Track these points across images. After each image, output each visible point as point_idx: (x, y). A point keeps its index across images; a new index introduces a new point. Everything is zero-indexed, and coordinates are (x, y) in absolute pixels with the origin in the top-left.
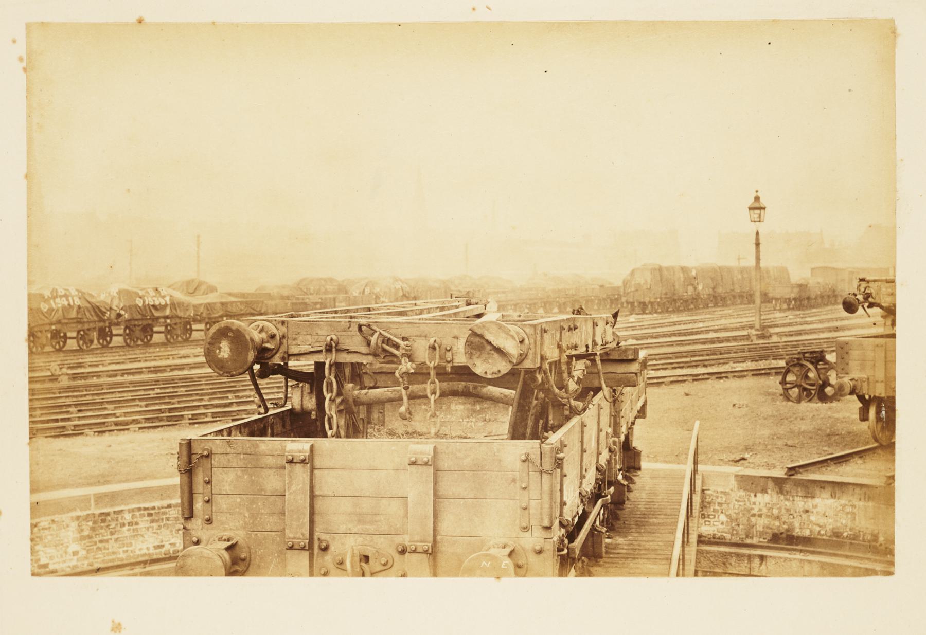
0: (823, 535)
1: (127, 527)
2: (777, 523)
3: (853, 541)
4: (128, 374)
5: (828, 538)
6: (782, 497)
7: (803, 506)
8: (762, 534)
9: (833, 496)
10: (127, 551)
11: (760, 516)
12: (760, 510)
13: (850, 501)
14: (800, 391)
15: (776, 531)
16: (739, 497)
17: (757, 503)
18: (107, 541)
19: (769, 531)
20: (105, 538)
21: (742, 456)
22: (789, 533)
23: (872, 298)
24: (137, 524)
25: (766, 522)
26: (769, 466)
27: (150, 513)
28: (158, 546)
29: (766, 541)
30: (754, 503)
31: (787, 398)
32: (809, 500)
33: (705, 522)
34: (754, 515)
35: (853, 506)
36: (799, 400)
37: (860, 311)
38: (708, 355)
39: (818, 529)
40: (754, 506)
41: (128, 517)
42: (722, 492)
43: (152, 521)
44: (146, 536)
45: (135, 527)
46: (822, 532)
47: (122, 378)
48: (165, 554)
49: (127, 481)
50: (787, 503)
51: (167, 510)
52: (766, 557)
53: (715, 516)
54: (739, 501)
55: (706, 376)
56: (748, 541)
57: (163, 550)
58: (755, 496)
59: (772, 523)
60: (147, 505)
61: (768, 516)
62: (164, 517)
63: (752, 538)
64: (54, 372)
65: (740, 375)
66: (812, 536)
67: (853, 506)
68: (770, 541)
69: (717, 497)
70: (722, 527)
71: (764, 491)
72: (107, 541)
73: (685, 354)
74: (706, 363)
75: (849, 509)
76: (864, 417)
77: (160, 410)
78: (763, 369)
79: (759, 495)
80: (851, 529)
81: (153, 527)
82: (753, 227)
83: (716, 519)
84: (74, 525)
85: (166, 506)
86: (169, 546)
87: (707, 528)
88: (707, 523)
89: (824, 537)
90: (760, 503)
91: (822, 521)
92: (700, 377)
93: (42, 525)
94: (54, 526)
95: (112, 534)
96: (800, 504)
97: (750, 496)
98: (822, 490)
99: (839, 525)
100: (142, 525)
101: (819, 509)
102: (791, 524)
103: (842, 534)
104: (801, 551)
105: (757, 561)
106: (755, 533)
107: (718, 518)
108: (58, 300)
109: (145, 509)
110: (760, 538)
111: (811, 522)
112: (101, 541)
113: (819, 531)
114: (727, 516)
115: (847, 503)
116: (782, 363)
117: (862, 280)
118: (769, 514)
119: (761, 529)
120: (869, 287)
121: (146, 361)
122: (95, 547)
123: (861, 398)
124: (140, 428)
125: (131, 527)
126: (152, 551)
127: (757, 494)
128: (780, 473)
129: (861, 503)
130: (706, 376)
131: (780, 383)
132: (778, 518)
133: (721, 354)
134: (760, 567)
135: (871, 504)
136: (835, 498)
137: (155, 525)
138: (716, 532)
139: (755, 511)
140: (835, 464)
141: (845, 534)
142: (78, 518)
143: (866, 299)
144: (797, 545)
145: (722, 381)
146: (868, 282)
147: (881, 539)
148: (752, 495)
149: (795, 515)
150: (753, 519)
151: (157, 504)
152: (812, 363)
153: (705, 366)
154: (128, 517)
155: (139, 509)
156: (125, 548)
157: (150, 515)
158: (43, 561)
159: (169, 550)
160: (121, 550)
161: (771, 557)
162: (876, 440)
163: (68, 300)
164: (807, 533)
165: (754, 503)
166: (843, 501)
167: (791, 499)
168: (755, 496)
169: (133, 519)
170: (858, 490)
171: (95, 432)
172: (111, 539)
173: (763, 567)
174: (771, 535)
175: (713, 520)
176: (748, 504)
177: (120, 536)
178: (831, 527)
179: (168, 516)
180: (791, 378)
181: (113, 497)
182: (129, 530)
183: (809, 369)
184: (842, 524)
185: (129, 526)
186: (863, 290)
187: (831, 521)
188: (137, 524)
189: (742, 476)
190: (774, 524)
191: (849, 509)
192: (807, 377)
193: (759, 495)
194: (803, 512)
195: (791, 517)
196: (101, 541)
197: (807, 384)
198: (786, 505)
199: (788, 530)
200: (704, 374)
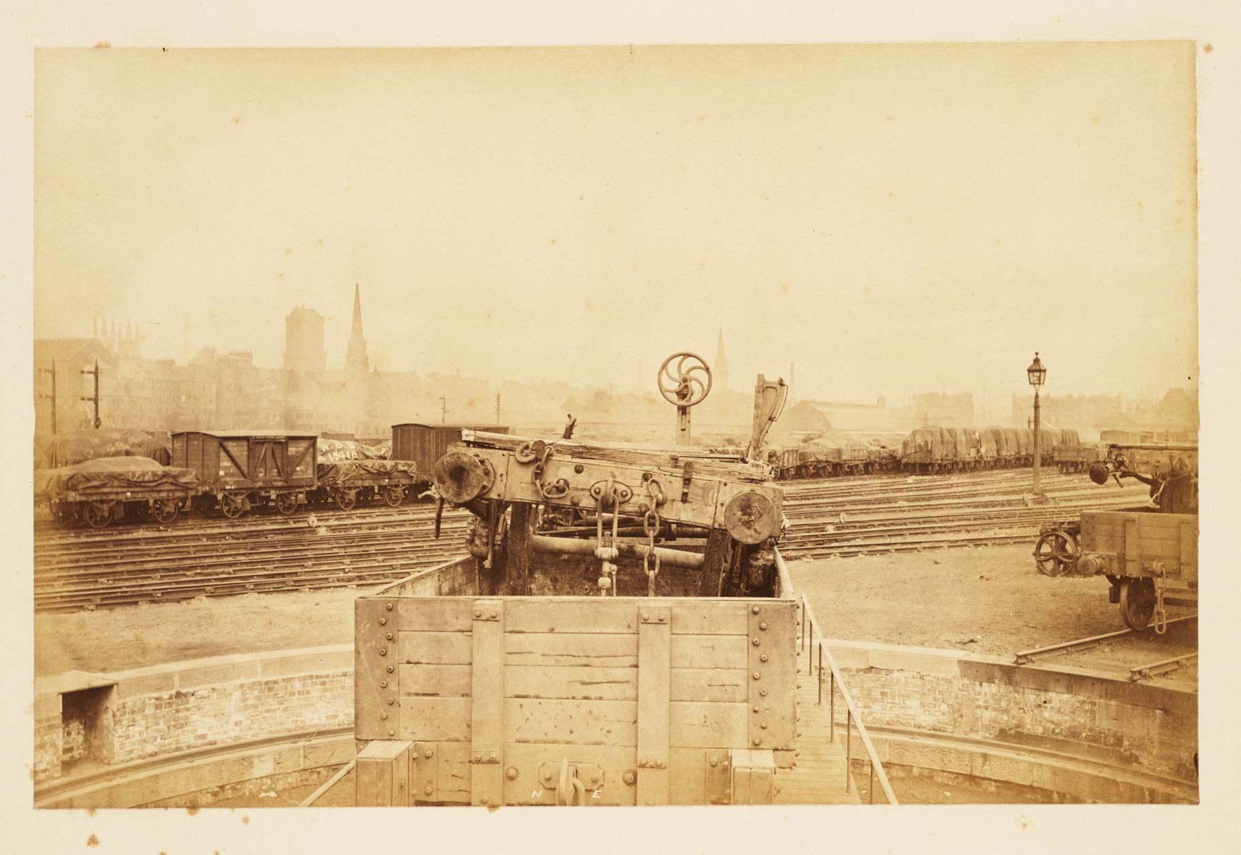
0: (1058, 734)
1: (297, 696)
2: (1005, 717)
3: (1092, 744)
4: (388, 526)
5: (1063, 738)
6: (1011, 688)
7: (1035, 701)
8: (988, 728)
9: (1070, 690)
10: (297, 721)
11: (986, 708)
12: (986, 701)
13: (1089, 697)
14: (1055, 564)
15: (1004, 726)
16: (963, 685)
17: (983, 693)
18: (274, 711)
19: (997, 725)
20: (274, 707)
21: (972, 638)
22: (1018, 730)
23: (1125, 466)
24: (308, 693)
25: (993, 715)
26: (998, 650)
27: (323, 680)
28: (332, 716)
29: (992, 736)
30: (980, 694)
31: (1041, 571)
32: (1043, 693)
33: (925, 710)
34: (979, 707)
35: (1093, 704)
36: (1054, 574)
37: (1111, 480)
38: (975, 519)
39: (1052, 726)
40: (979, 697)
41: (298, 685)
42: (943, 679)
43: (326, 690)
44: (318, 706)
45: (305, 696)
46: (1057, 731)
47: (383, 531)
48: (339, 725)
49: (306, 645)
50: (1016, 695)
51: (343, 678)
52: (990, 755)
53: (935, 705)
54: (962, 690)
55: (965, 543)
56: (972, 736)
57: (337, 721)
58: (981, 685)
59: (1000, 717)
60: (319, 673)
61: (995, 709)
62: (339, 686)
63: (977, 731)
64: (311, 524)
65: (1001, 542)
66: (1046, 735)
67: (1093, 704)
68: (997, 737)
69: (938, 684)
70: (943, 717)
71: (991, 680)
72: (274, 711)
73: (951, 518)
74: (969, 528)
75: (1088, 707)
76: (1115, 598)
77: (392, 566)
78: (1028, 537)
79: (985, 684)
80: (1090, 730)
81: (326, 697)
82: (1031, 391)
83: (937, 709)
84: (237, 694)
85: (341, 674)
86: (344, 717)
87: (927, 718)
88: (927, 713)
89: (1060, 737)
90: (986, 693)
91: (1056, 718)
92: (958, 544)
93: (204, 693)
94: (214, 695)
95: (281, 703)
96: (1031, 697)
97: (975, 685)
98: (1057, 683)
99: (1076, 724)
100: (314, 693)
101: (1053, 704)
102: (1021, 719)
103: (1080, 734)
104: (1031, 752)
105: (980, 760)
106: (980, 726)
107: (939, 707)
108: (335, 454)
109: (318, 677)
110: (986, 732)
111: (1045, 718)
112: (268, 711)
113: (1054, 730)
114: (948, 705)
115: (1085, 699)
116: (1036, 531)
117: (1113, 446)
118: (996, 706)
119: (987, 723)
120: (1121, 454)
121: (414, 513)
122: (260, 717)
123: (1111, 578)
124: (358, 585)
125: (302, 697)
126: (324, 721)
127: (983, 684)
128: (1008, 660)
129: (1102, 701)
130: (965, 543)
131: (1034, 554)
132: (1006, 711)
133: (989, 519)
134: (983, 767)
135: (1113, 703)
136: (1071, 694)
137: (328, 694)
138: (936, 723)
139: (981, 703)
140: (1077, 651)
141: (1084, 735)
142: (242, 686)
143: (1117, 468)
144: (1027, 744)
145: (979, 548)
146: (1120, 448)
147: (1126, 743)
148: (978, 684)
149: (1026, 709)
150: (979, 712)
151: (330, 672)
152: (1070, 534)
153: (968, 531)
154: (298, 685)
155: (311, 677)
156: (295, 719)
157: (323, 683)
158: (200, 732)
159: (343, 721)
160: (289, 720)
161: (995, 756)
162: (1129, 625)
163: (345, 454)
164: (1040, 730)
165: (980, 694)
166: (1081, 698)
167: (1021, 691)
168: (981, 685)
169: (303, 687)
170: (1097, 686)
171: (310, 589)
172: (279, 709)
173: (987, 767)
174: (998, 731)
175: (933, 709)
176: (972, 693)
177: (289, 705)
178: (1067, 725)
179: (343, 684)
180: (1046, 549)
181: (285, 662)
182: (298, 699)
183: (1066, 541)
184: (1080, 722)
185: (299, 694)
186: (1114, 457)
187: (1067, 718)
188: (308, 693)
189: (966, 662)
190: (1002, 718)
191: (1088, 707)
192: (1063, 549)
193: (985, 684)
194: (1035, 706)
195: (1022, 711)
196: (268, 711)
197: (1063, 556)
198: (1015, 698)
199: (1018, 726)
200: (963, 540)
